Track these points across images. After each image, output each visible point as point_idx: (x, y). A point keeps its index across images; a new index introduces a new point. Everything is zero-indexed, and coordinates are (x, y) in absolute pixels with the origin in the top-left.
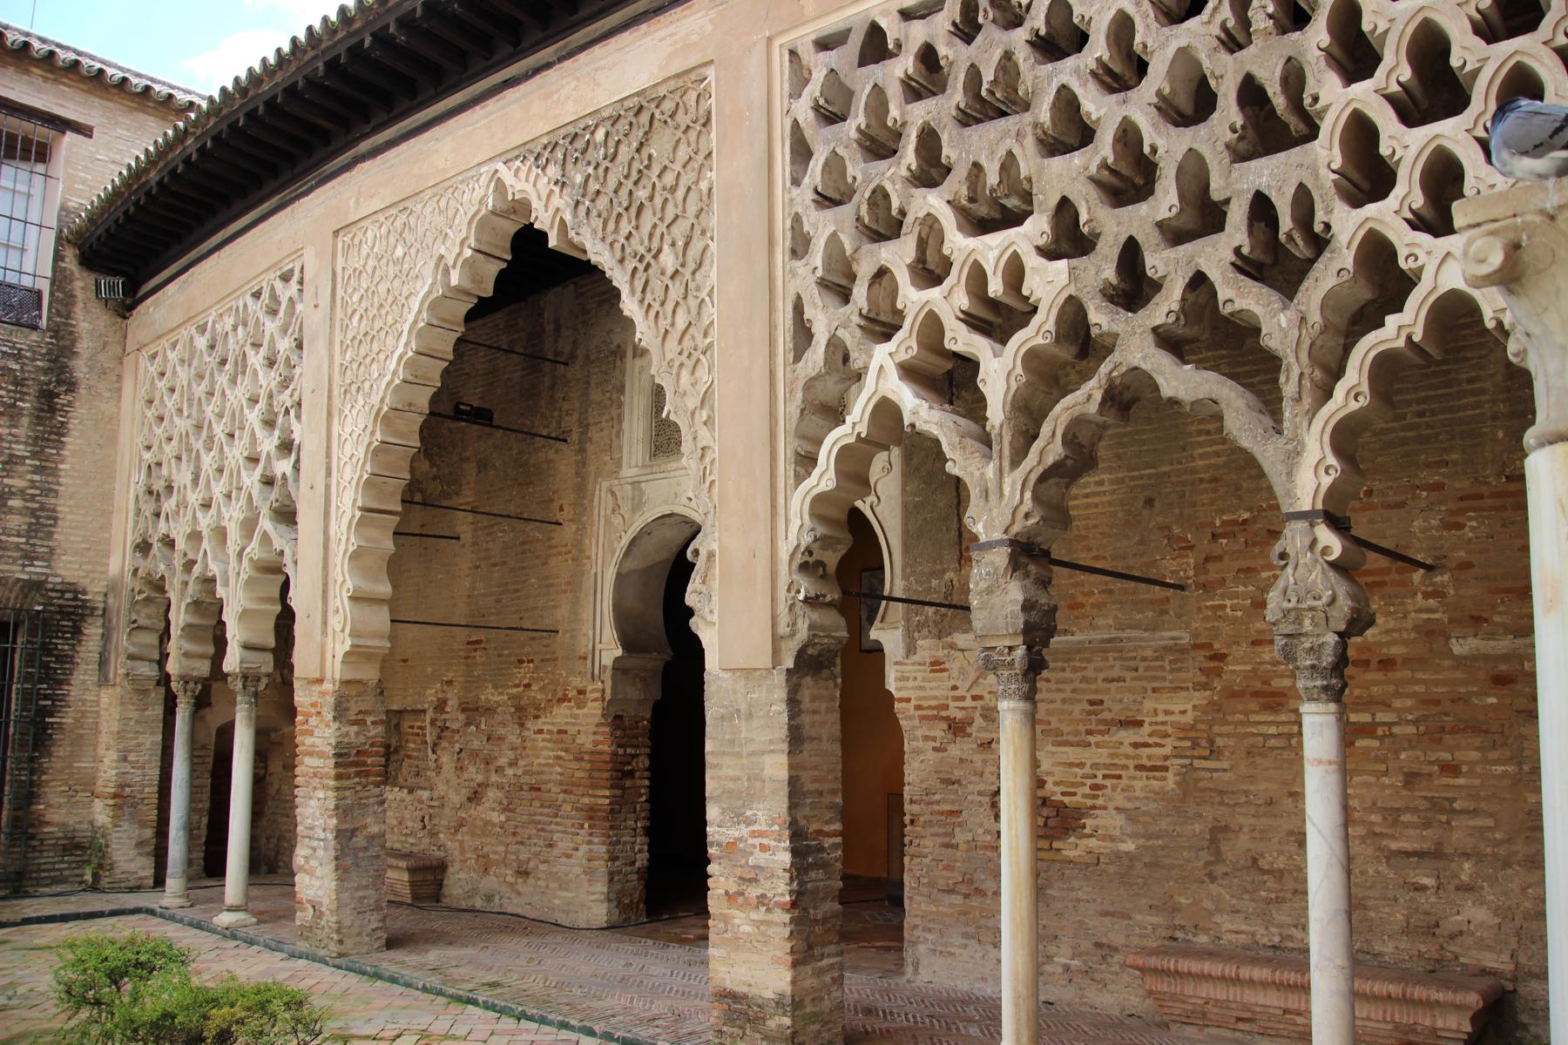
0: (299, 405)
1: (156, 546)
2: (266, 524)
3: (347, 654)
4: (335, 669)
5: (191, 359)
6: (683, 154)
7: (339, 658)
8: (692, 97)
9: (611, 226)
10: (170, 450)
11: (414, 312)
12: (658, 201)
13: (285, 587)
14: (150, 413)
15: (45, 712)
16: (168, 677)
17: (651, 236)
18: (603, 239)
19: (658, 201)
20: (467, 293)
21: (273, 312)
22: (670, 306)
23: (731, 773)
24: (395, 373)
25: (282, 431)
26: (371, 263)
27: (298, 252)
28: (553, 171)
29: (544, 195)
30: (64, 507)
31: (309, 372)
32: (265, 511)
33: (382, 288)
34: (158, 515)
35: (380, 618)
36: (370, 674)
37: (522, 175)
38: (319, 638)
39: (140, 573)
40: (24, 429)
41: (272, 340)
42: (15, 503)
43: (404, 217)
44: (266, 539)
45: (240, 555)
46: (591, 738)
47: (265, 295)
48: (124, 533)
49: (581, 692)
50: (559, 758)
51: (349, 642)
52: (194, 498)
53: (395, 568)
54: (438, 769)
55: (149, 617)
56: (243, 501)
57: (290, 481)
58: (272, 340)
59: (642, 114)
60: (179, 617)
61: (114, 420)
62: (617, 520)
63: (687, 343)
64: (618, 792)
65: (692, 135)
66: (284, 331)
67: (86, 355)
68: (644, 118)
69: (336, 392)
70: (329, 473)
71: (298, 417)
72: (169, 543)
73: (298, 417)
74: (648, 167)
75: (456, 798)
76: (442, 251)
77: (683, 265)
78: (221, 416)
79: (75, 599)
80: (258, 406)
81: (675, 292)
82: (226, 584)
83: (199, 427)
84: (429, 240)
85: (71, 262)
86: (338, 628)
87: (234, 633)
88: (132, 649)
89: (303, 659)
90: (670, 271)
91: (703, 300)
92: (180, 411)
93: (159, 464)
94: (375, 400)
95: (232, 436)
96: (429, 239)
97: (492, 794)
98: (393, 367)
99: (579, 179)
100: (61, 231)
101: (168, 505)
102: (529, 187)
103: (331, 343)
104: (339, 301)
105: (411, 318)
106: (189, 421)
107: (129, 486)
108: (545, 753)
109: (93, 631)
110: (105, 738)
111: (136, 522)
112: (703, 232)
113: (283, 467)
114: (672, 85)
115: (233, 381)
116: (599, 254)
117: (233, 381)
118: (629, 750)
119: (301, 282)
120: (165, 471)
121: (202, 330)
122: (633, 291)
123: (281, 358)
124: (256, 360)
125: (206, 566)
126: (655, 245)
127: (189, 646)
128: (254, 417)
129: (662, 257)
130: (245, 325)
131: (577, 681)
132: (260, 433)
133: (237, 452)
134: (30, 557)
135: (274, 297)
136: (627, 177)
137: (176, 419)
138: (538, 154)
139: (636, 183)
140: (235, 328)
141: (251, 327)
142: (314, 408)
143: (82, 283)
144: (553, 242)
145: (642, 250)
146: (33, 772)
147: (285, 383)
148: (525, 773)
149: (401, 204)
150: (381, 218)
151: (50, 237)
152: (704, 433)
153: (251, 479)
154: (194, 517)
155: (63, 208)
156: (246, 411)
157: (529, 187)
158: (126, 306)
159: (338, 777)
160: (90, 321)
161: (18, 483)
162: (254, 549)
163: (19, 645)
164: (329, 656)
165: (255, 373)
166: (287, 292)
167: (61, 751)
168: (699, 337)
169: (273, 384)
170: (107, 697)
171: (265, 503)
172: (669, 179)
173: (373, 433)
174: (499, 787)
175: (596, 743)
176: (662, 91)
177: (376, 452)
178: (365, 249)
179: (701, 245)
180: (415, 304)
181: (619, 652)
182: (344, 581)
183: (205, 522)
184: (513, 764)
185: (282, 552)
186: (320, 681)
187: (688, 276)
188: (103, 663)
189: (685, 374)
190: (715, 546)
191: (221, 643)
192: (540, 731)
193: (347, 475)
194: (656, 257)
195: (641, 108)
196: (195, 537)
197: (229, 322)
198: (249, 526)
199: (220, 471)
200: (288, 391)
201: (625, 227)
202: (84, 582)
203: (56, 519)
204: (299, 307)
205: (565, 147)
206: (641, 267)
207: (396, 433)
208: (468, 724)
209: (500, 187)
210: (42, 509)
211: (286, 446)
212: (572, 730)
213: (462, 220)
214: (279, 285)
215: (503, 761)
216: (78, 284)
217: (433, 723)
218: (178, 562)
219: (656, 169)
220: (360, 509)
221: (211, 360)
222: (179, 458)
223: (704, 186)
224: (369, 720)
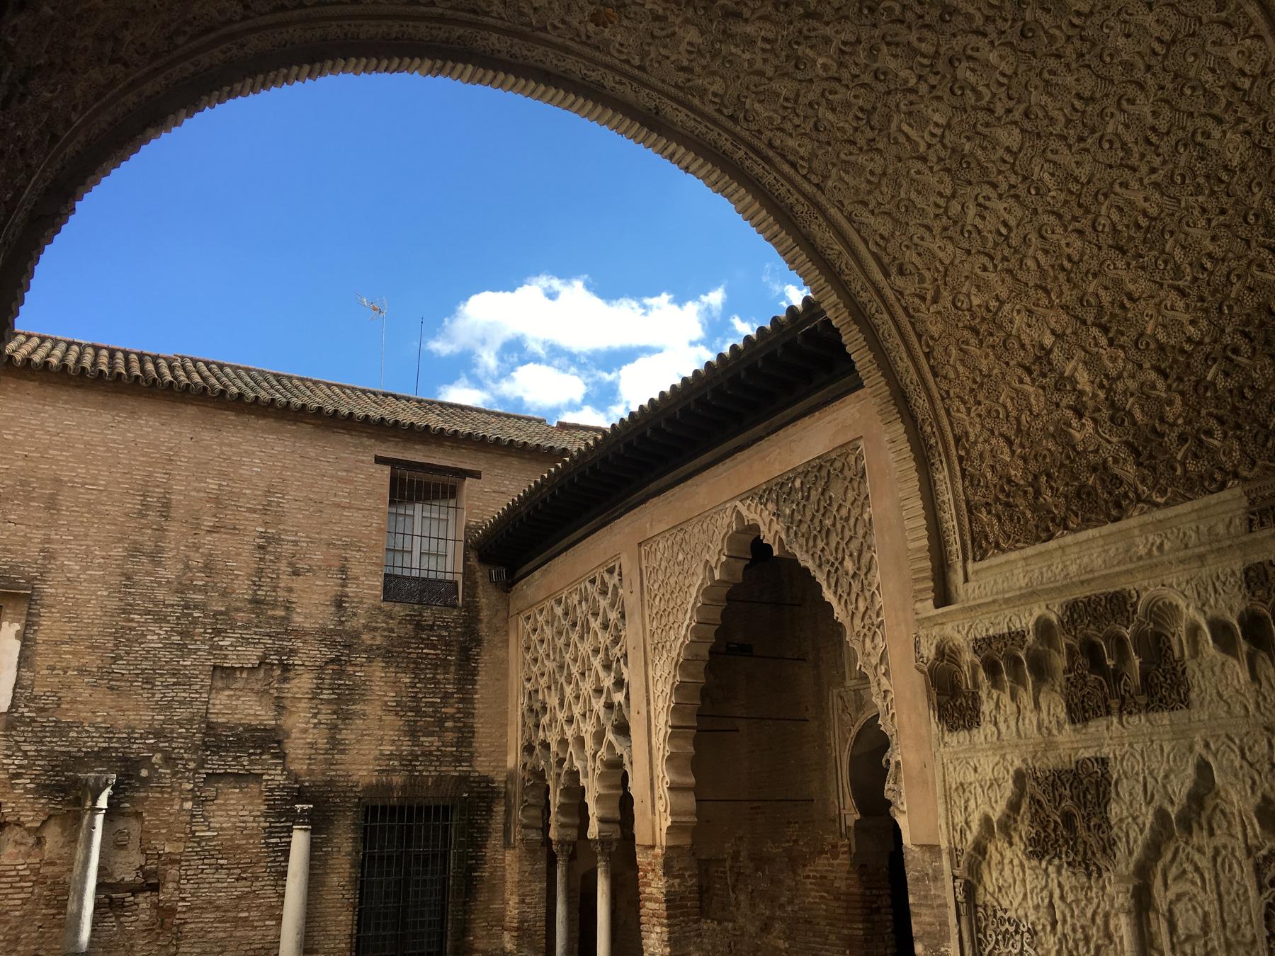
0: (626, 655)
1: (538, 748)
2: (610, 736)
3: (669, 828)
4: (662, 839)
6: (851, 495)
7: (664, 831)
8: (852, 458)
9: (811, 543)
10: (543, 682)
11: (693, 596)
12: (839, 526)
13: (625, 777)
15: (473, 869)
16: (549, 841)
17: (837, 549)
18: (807, 552)
19: (839, 526)
20: (725, 582)
21: (604, 593)
22: (853, 596)
23: (927, 919)
24: (685, 636)
26: (664, 564)
27: (617, 557)
29: (767, 521)
30: (478, 724)
31: (632, 633)
32: (609, 727)
33: (672, 580)
34: (537, 726)
35: (689, 801)
36: (685, 841)
37: (753, 509)
38: (650, 816)
42: (449, 724)
44: (611, 746)
45: (594, 756)
46: (844, 883)
47: (598, 582)
48: (515, 739)
49: (834, 846)
50: (822, 897)
51: (670, 819)
52: (561, 716)
53: (698, 764)
54: (738, 904)
55: (534, 797)
56: (594, 720)
59: (822, 471)
60: (555, 799)
61: (505, 661)
62: (846, 718)
63: (867, 621)
64: (869, 925)
65: (855, 484)
66: (613, 605)
67: (486, 620)
68: (824, 473)
69: (648, 648)
70: (648, 704)
71: (626, 664)
72: (546, 746)
73: (626, 664)
74: (830, 505)
75: (752, 929)
77: (859, 569)
78: (575, 660)
79: (488, 786)
81: (856, 587)
82: (586, 776)
83: (561, 667)
85: (473, 562)
86: (662, 809)
87: (593, 810)
88: (525, 821)
89: (641, 833)
90: (851, 572)
92: (548, 655)
93: (537, 691)
94: (674, 654)
95: (583, 674)
96: (699, 550)
97: (778, 926)
98: (683, 633)
99: (788, 511)
100: (466, 542)
101: (545, 720)
102: (757, 517)
103: (643, 616)
105: (692, 601)
106: (555, 664)
108: (813, 894)
109: (500, 809)
110: (509, 886)
111: (523, 732)
112: (869, 547)
113: (618, 697)
114: (839, 452)
115: (582, 638)
116: (805, 561)
117: (582, 638)
118: (874, 892)
119: (620, 574)
120: (540, 697)
121: (559, 602)
122: (829, 586)
124: (595, 624)
126: (840, 556)
127: (562, 819)
128: (597, 663)
129: (845, 563)
130: (587, 601)
131: (830, 838)
132: (602, 674)
134: (458, 760)
135: (603, 583)
136: (817, 511)
138: (761, 495)
139: (823, 515)
140: (580, 603)
141: (591, 601)
142: (635, 657)
143: (480, 574)
144: (776, 553)
145: (832, 559)
146: (465, 912)
147: (616, 641)
148: (800, 909)
149: (679, 527)
151: (461, 546)
152: (884, 680)
153: (598, 705)
155: (467, 527)
157: (757, 517)
158: (508, 584)
159: (668, 917)
160: (486, 598)
161: (451, 710)
163: (454, 823)
164: (657, 829)
165: (596, 633)
166: (612, 581)
167: (482, 897)
168: (874, 617)
169: (608, 642)
170: (509, 856)
172: (844, 512)
173: (674, 676)
174: (783, 920)
175: (848, 886)
176: (833, 456)
177: (677, 689)
178: (659, 555)
179: (869, 555)
180: (694, 591)
181: (858, 816)
182: (664, 777)
183: (570, 732)
184: (790, 902)
186: (653, 847)
188: (507, 832)
189: (868, 641)
190: (899, 758)
192: (808, 877)
193: (660, 704)
194: (841, 563)
195: (821, 467)
196: (563, 743)
197: (576, 598)
198: (599, 736)
199: (577, 697)
201: (820, 544)
202: (492, 774)
203: (473, 732)
204: (621, 591)
205: (775, 491)
207: (688, 675)
208: (756, 870)
209: (739, 516)
210: (465, 726)
212: (831, 876)
213: (718, 538)
214: (606, 576)
215: (784, 899)
216: (479, 574)
217: (731, 868)
218: (553, 760)
219: (835, 506)
221: (566, 623)
223: (866, 516)
224: (687, 874)
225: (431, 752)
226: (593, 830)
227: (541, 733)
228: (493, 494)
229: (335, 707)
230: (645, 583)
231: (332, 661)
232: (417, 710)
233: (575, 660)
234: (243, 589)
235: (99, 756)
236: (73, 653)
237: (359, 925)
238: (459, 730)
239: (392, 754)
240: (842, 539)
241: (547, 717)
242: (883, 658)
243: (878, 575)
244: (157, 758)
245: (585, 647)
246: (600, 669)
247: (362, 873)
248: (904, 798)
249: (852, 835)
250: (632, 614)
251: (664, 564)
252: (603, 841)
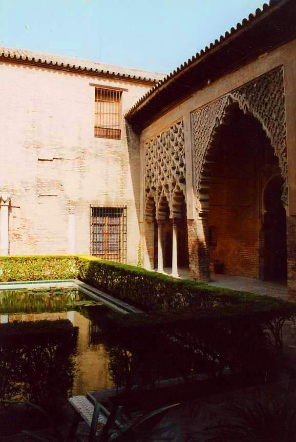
0: (184, 155)
1: (151, 189)
2: (178, 184)
5: (157, 143)
6: (277, 88)
8: (278, 74)
14: (147, 157)
17: (269, 110)
18: (257, 111)
21: (176, 132)
24: (208, 146)
26: (200, 120)
28: (244, 95)
32: (177, 180)
33: (203, 125)
34: (151, 182)
37: (236, 96)
39: (148, 196)
43: (207, 108)
44: (178, 188)
45: (172, 191)
47: (174, 128)
52: (160, 177)
60: (158, 206)
63: (280, 137)
66: (179, 136)
71: (184, 158)
72: (154, 188)
73: (184, 158)
76: (217, 116)
80: (174, 155)
83: (160, 161)
84: (214, 113)
87: (171, 209)
91: (283, 126)
92: (155, 156)
93: (150, 170)
94: (203, 153)
95: (168, 162)
101: (153, 179)
104: (192, 129)
105: (211, 133)
111: (146, 184)
113: (181, 169)
116: (256, 115)
119: (183, 125)
120: (152, 171)
121: (159, 137)
122: (265, 125)
125: (164, 194)
126: (270, 113)
127: (160, 213)
128: (173, 158)
129: (273, 116)
133: (170, 166)
139: (265, 97)
147: (181, 150)
149: (207, 105)
150: (202, 108)
152: (284, 158)
153: (174, 173)
156: (171, 157)
162: (175, 190)
165: (173, 147)
166: (179, 127)
171: (177, 178)
172: (273, 96)
173: (203, 161)
180: (211, 129)
183: (163, 183)
187: (279, 120)
189: (279, 144)
190: (288, 186)
194: (271, 115)
198: (174, 184)
200: (182, 152)
204: (183, 131)
205: (245, 89)
206: (267, 118)
209: (231, 99)
211: (182, 165)
214: (177, 125)
218: (157, 193)
220: (201, 179)
221: (161, 144)
222: (155, 168)
223: (282, 97)
226: (171, 217)
227: (152, 184)
228: (133, 96)
230: (193, 127)
240: (272, 106)
241: (155, 178)
242: (285, 150)
243: (286, 119)
245: (168, 153)
248: (288, 200)
249: (263, 217)
250: (187, 139)
251: (200, 120)
252: (175, 219)
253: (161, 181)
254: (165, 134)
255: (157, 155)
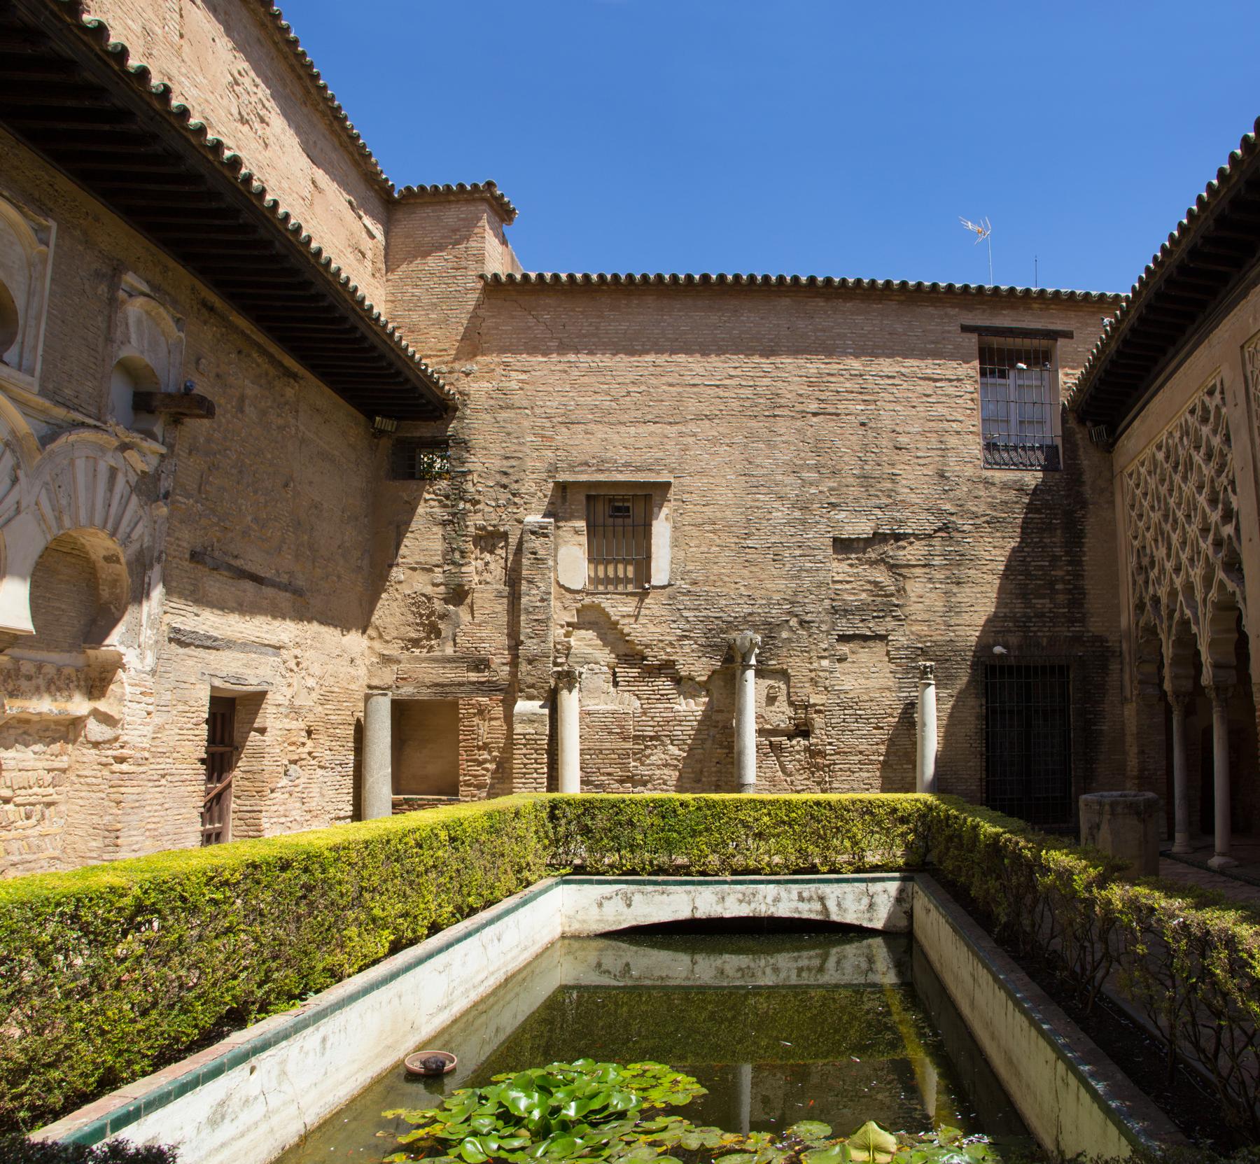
0: (1232, 482)
2: (1220, 575)
13: (1239, 619)
25: (1224, 504)
34: (1147, 582)
39: (1141, 624)
40: (1058, 537)
41: (1208, 440)
42: (1059, 587)
45: (1205, 600)
48: (1127, 599)
52: (1169, 566)
57: (1234, 539)
58: (1208, 440)
60: (1168, 651)
71: (1234, 492)
72: (1156, 600)
73: (1234, 492)
83: (1166, 517)
92: (1152, 508)
93: (1144, 547)
101: (1153, 574)
107: (1127, 564)
109: (1114, 666)
115: (1185, 479)
117: (1185, 479)
120: (1148, 551)
121: (1159, 448)
123: (1216, 452)
124: (1198, 458)
128: (1202, 500)
130: (1188, 435)
132: (1208, 510)
134: (1072, 621)
137: (1152, 514)
140: (1181, 439)
141: (1192, 436)
147: (1219, 472)
153: (1206, 546)
154: (1171, 579)
161: (1060, 573)
165: (1200, 467)
169: (1213, 473)
171: (1218, 559)
183: (1178, 582)
185: (1234, 593)
191: (1198, 667)
203: (1084, 594)
211: (1228, 515)
218: (1164, 613)
221: (1168, 467)
225: (1043, 615)
226: (1207, 678)
229: (948, 573)
231: (940, 530)
232: (1028, 574)
233: (1179, 505)
234: (850, 466)
235: (747, 621)
236: (714, 532)
237: (987, 770)
238: (1069, 592)
239: (1005, 616)
241: (1156, 570)
244: (794, 622)
245: (1189, 488)
246: (1205, 505)
247: (987, 724)
253: (1174, 576)
254: (1177, 435)
255: (1159, 502)
